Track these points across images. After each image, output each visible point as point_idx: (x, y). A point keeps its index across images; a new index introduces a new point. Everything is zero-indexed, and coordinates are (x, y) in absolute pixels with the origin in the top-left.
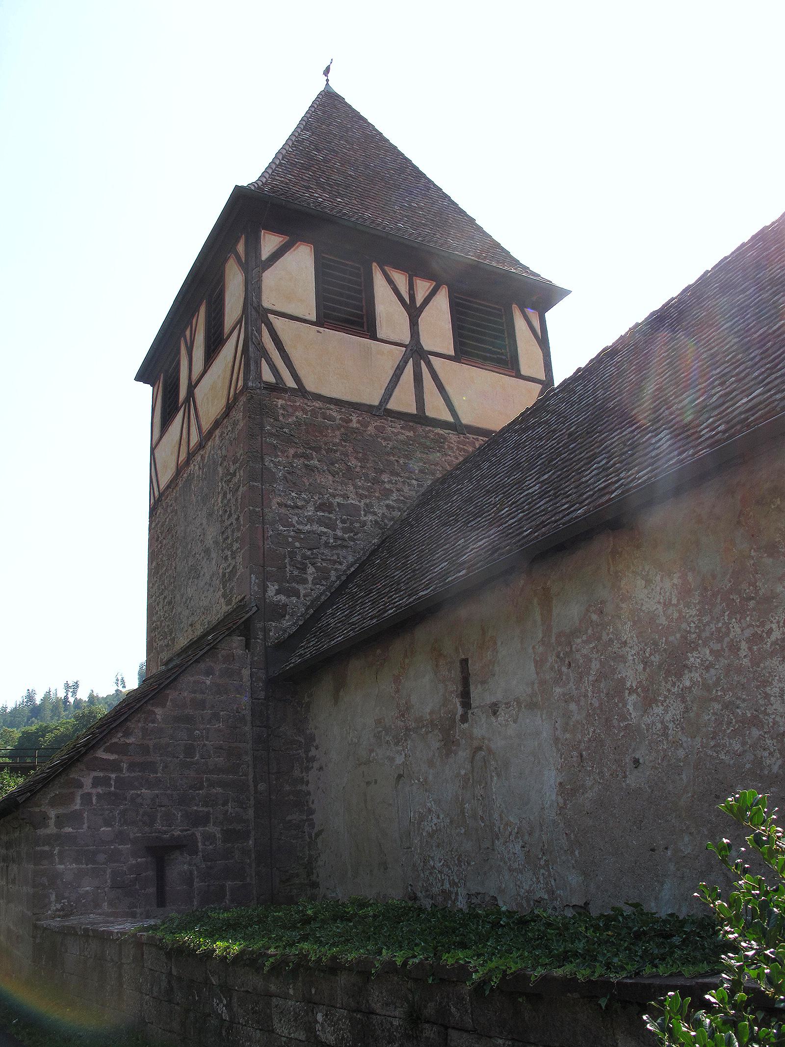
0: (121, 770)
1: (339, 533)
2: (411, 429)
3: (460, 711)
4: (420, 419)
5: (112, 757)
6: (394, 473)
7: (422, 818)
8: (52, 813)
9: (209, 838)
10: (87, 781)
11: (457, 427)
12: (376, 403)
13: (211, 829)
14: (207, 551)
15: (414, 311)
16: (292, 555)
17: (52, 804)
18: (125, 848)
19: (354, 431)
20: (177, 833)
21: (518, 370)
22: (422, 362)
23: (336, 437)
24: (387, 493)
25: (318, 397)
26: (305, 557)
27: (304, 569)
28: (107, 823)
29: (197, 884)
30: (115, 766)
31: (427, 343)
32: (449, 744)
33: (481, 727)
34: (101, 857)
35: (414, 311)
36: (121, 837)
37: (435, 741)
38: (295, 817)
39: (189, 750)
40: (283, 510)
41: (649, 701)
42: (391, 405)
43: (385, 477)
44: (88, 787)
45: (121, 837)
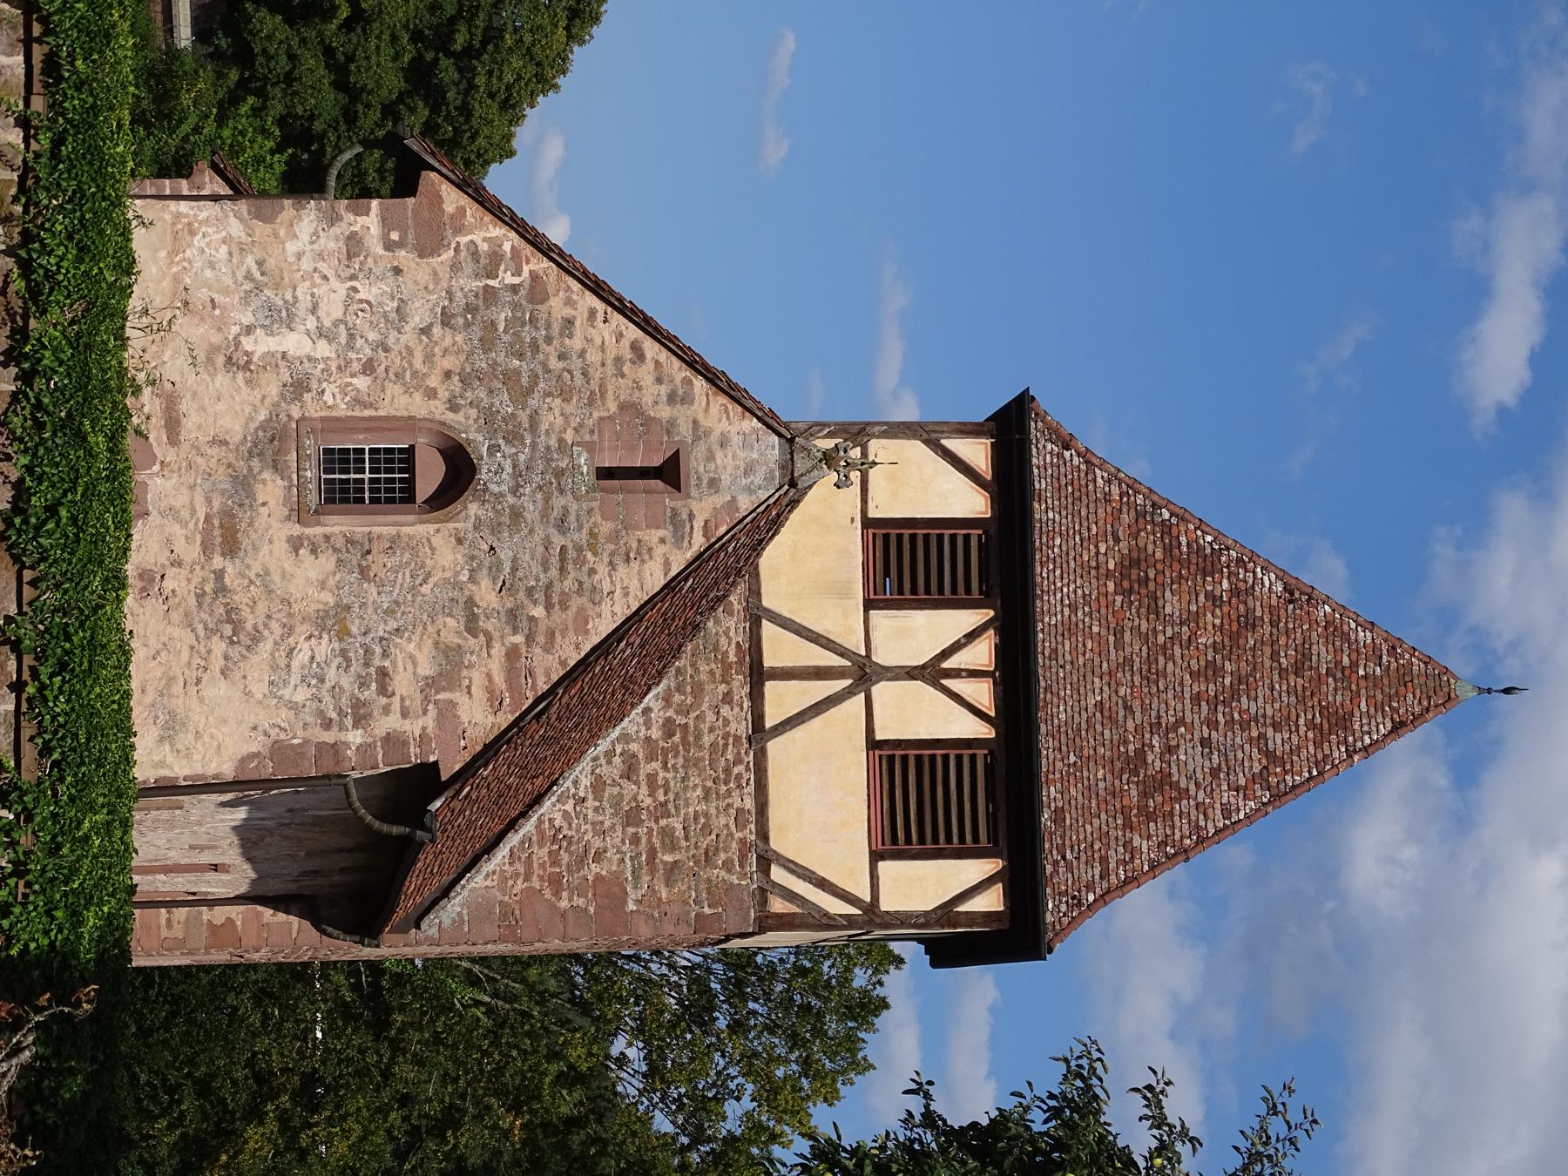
2: (740, 662)
4: (758, 675)
11: (759, 733)
12: (766, 603)
15: (933, 673)
21: (883, 858)
22: (849, 682)
31: (881, 691)
35: (933, 673)
42: (764, 622)
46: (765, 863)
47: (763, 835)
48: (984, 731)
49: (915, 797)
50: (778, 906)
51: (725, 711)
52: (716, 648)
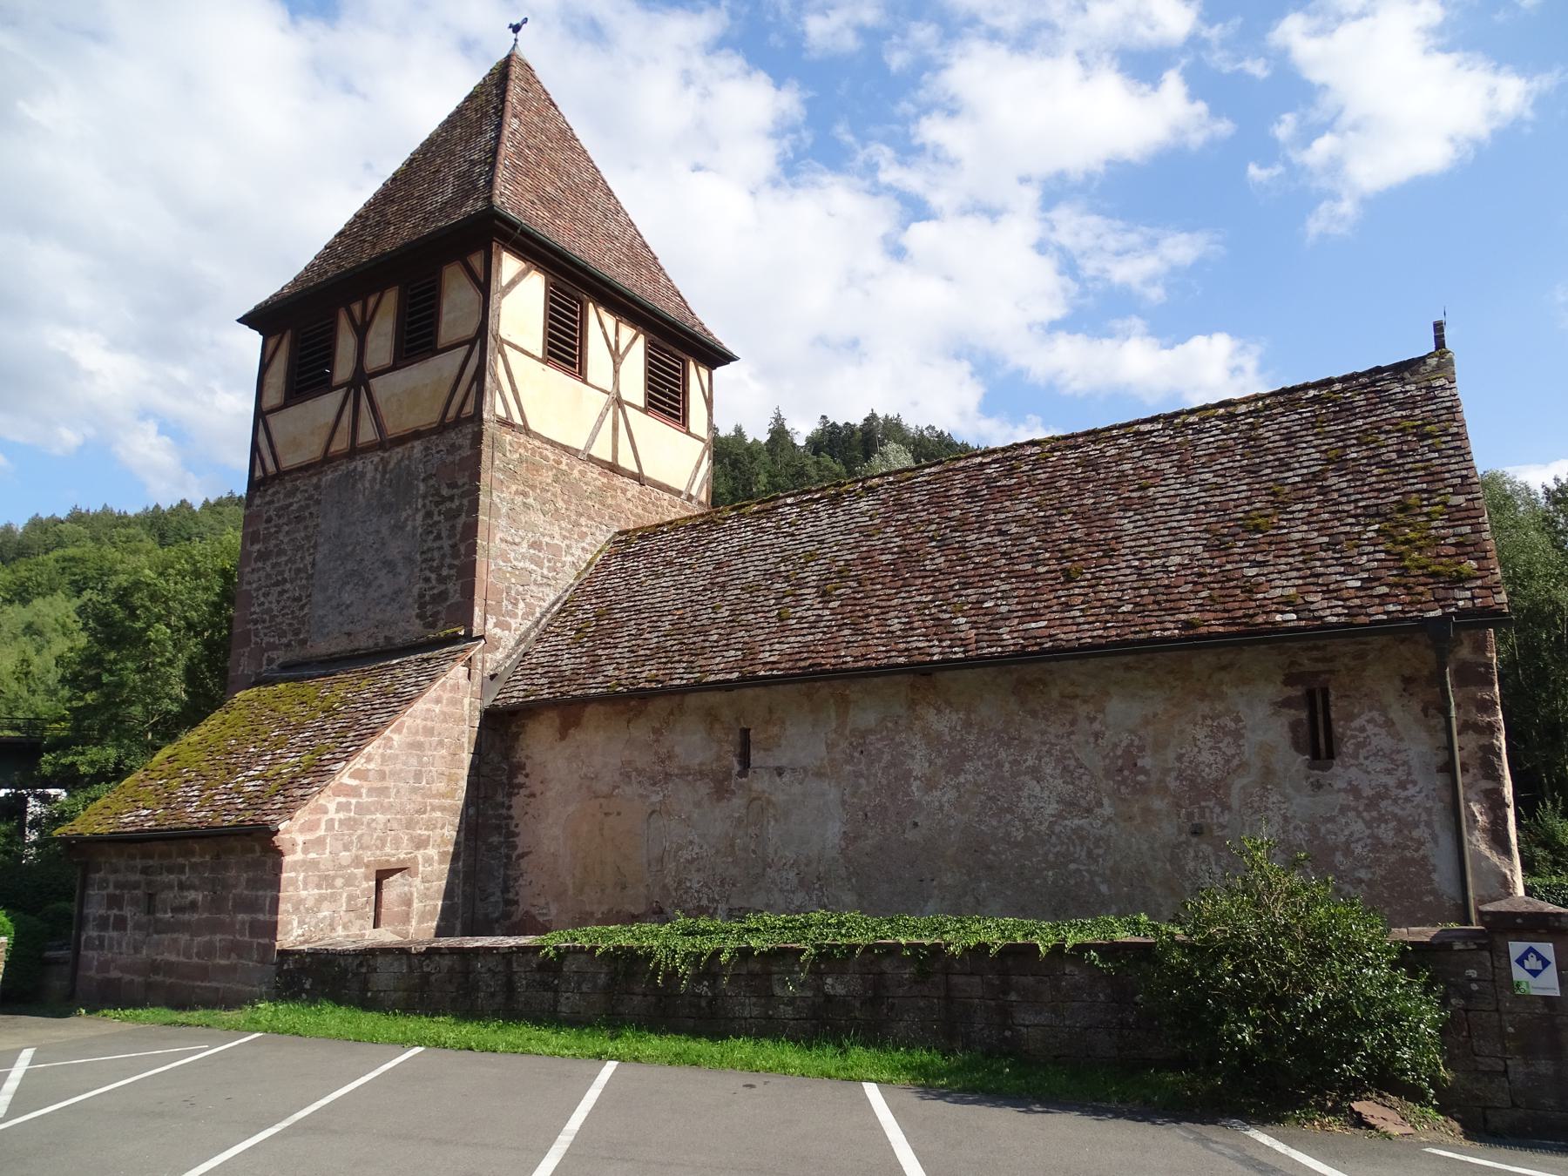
0: (360, 796)
1: (545, 571)
3: (737, 768)
4: (613, 468)
5: (354, 782)
6: (590, 518)
7: (680, 848)
8: (300, 839)
9: (429, 860)
10: (332, 807)
11: (639, 478)
13: (432, 852)
14: (389, 565)
16: (508, 589)
17: (302, 830)
18: (360, 871)
19: (564, 473)
20: (402, 856)
23: (548, 477)
24: (583, 536)
25: (538, 436)
26: (518, 593)
27: (515, 605)
28: (346, 848)
29: (416, 905)
30: (355, 792)
32: (721, 790)
33: (760, 783)
34: (339, 882)
35: (617, 356)
36: (357, 862)
37: (704, 788)
38: (495, 839)
39: (418, 776)
40: (504, 545)
41: (930, 784)
43: (583, 521)
44: (332, 814)
45: (357, 862)
46: (690, 498)
47: (679, 493)
48: (641, 338)
49: (666, 399)
50: (703, 497)
51: (629, 495)
52: (600, 489)
